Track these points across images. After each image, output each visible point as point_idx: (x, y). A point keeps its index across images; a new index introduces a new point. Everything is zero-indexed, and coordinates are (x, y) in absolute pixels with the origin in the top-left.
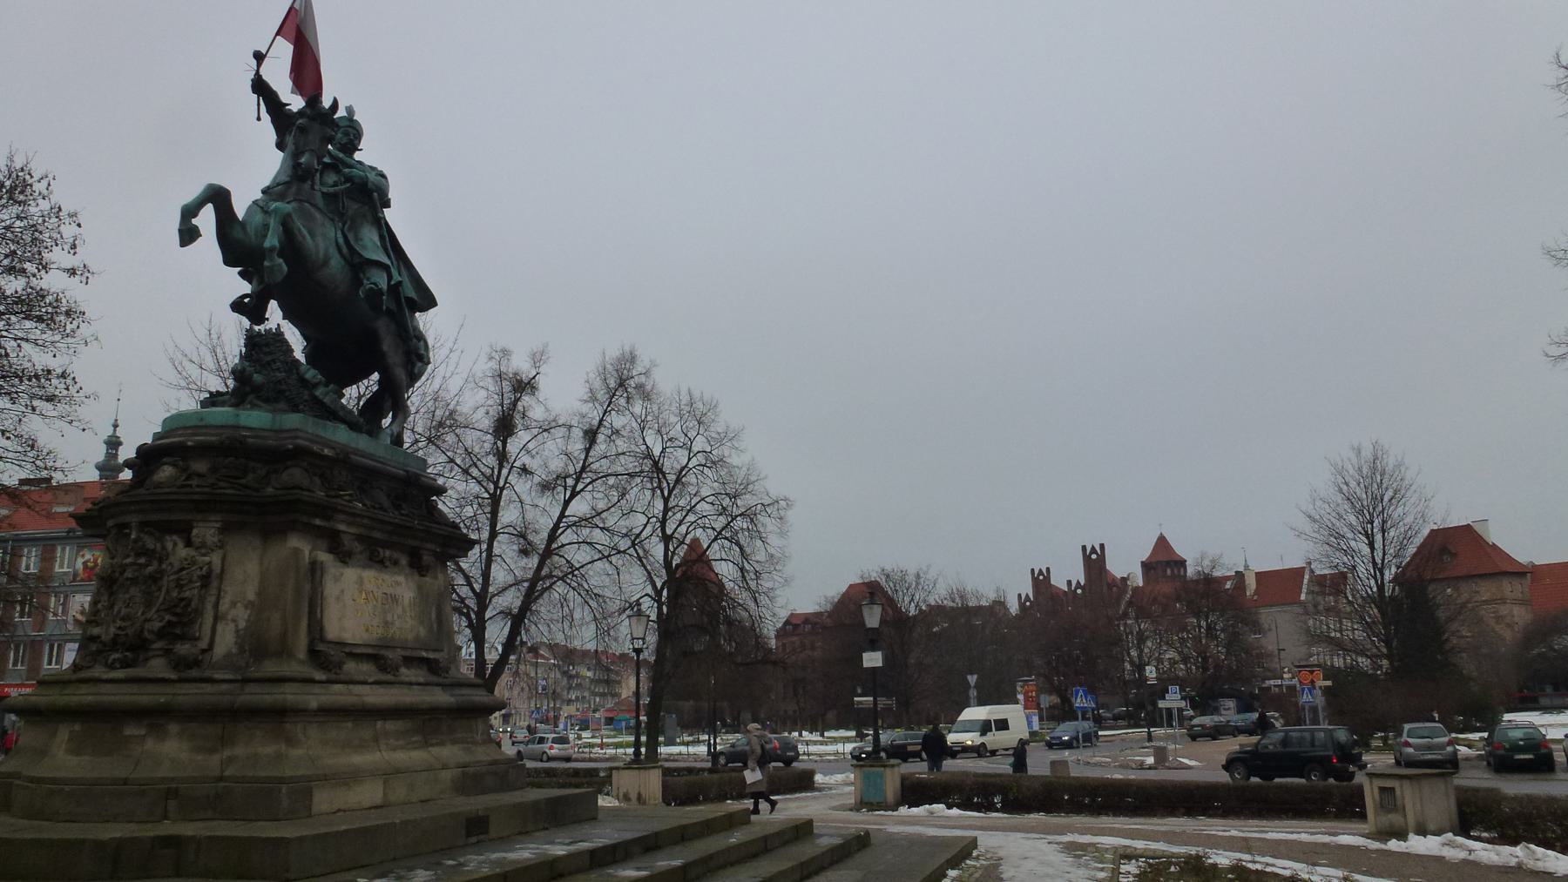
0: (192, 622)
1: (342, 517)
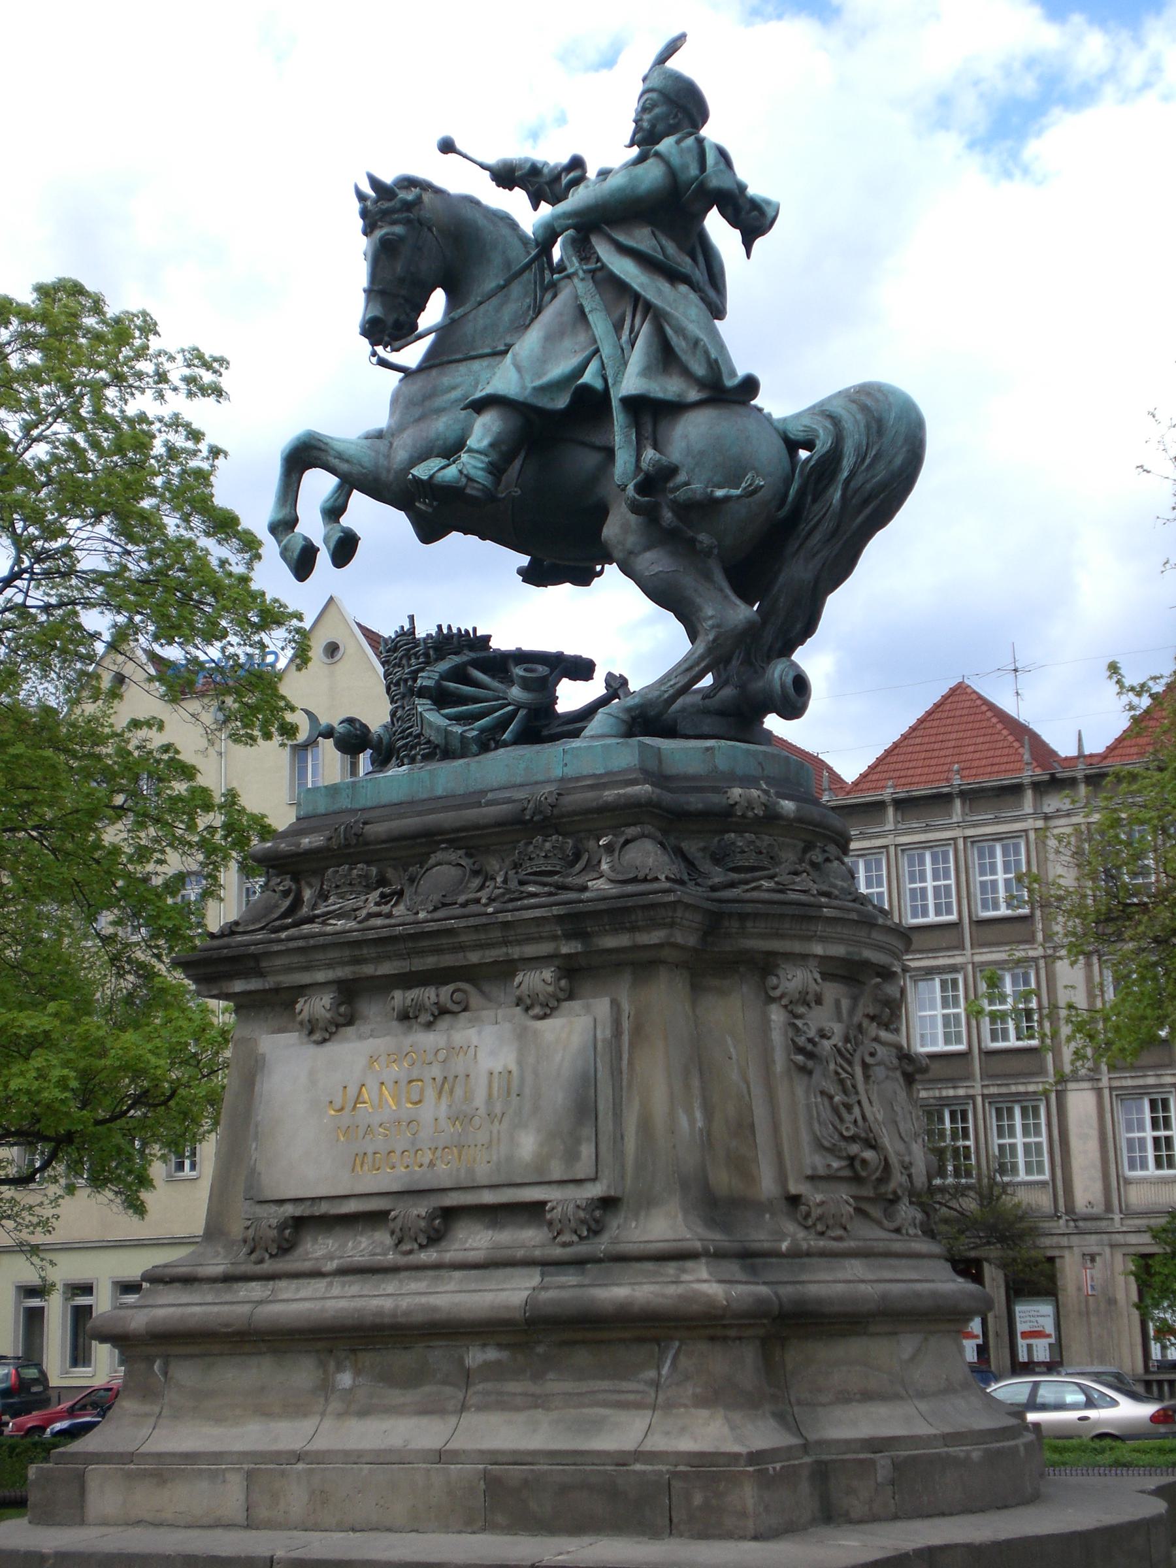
1: (279, 962)
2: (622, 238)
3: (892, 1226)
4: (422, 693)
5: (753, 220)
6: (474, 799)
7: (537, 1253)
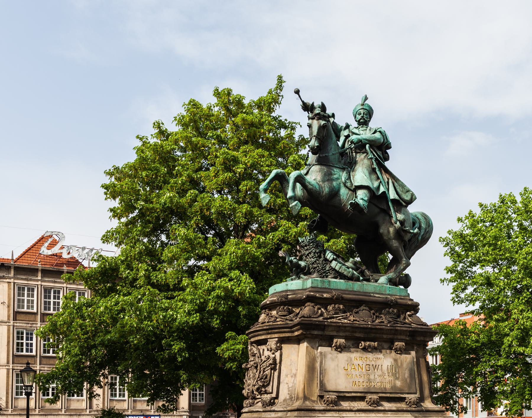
0: (268, 384)
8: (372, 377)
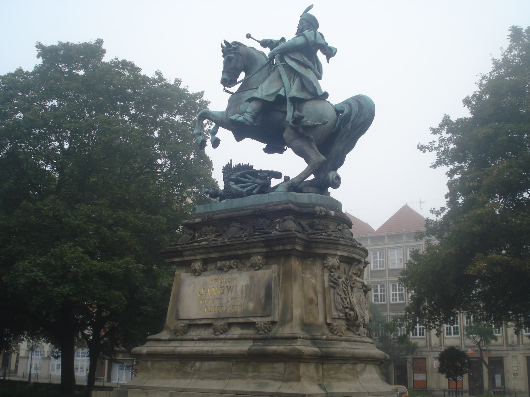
1: (186, 253)
2: (292, 56)
3: (357, 333)
4: (232, 180)
5: (330, 53)
6: (242, 209)
7: (252, 336)
8: (224, 300)
